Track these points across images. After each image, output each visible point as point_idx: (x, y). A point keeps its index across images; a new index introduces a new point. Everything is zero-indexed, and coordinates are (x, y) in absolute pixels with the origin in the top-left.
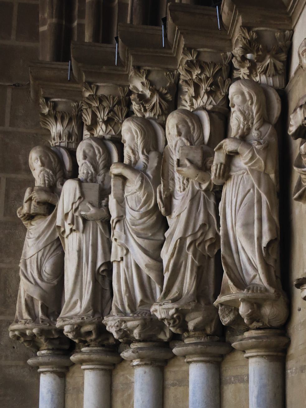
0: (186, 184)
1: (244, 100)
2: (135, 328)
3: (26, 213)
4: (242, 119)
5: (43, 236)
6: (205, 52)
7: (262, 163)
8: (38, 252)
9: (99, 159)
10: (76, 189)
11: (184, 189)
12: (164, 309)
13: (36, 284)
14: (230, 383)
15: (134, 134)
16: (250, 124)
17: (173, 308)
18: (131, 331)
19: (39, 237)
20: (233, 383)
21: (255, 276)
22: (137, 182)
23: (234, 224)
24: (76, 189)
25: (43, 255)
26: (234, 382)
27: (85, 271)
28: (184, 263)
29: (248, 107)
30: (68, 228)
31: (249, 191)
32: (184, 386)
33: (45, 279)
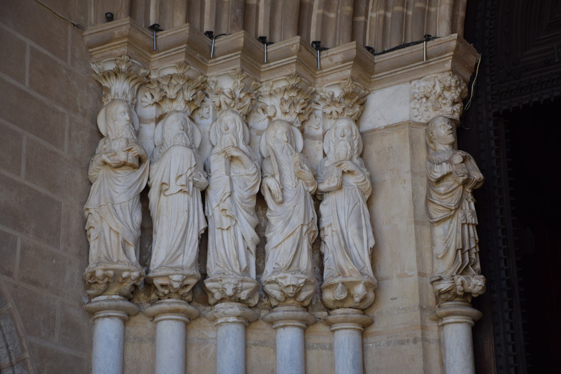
0: (297, 183)
1: (352, 135)
2: (247, 288)
3: (123, 161)
4: (349, 148)
5: (134, 187)
6: (304, 81)
7: (368, 185)
8: (129, 201)
9: (190, 133)
10: (191, 156)
11: (296, 187)
12: (297, 277)
13: (131, 231)
14: (313, 349)
15: (238, 125)
16: (353, 153)
17: (304, 278)
18: (242, 290)
19: (131, 187)
20: (316, 349)
21: (364, 267)
22: (253, 168)
23: (347, 225)
24: (191, 156)
25: (132, 205)
26: (317, 348)
27: (190, 230)
28: (301, 244)
29: (353, 140)
30: (174, 188)
31: (357, 203)
32: (266, 347)
33: (136, 228)
